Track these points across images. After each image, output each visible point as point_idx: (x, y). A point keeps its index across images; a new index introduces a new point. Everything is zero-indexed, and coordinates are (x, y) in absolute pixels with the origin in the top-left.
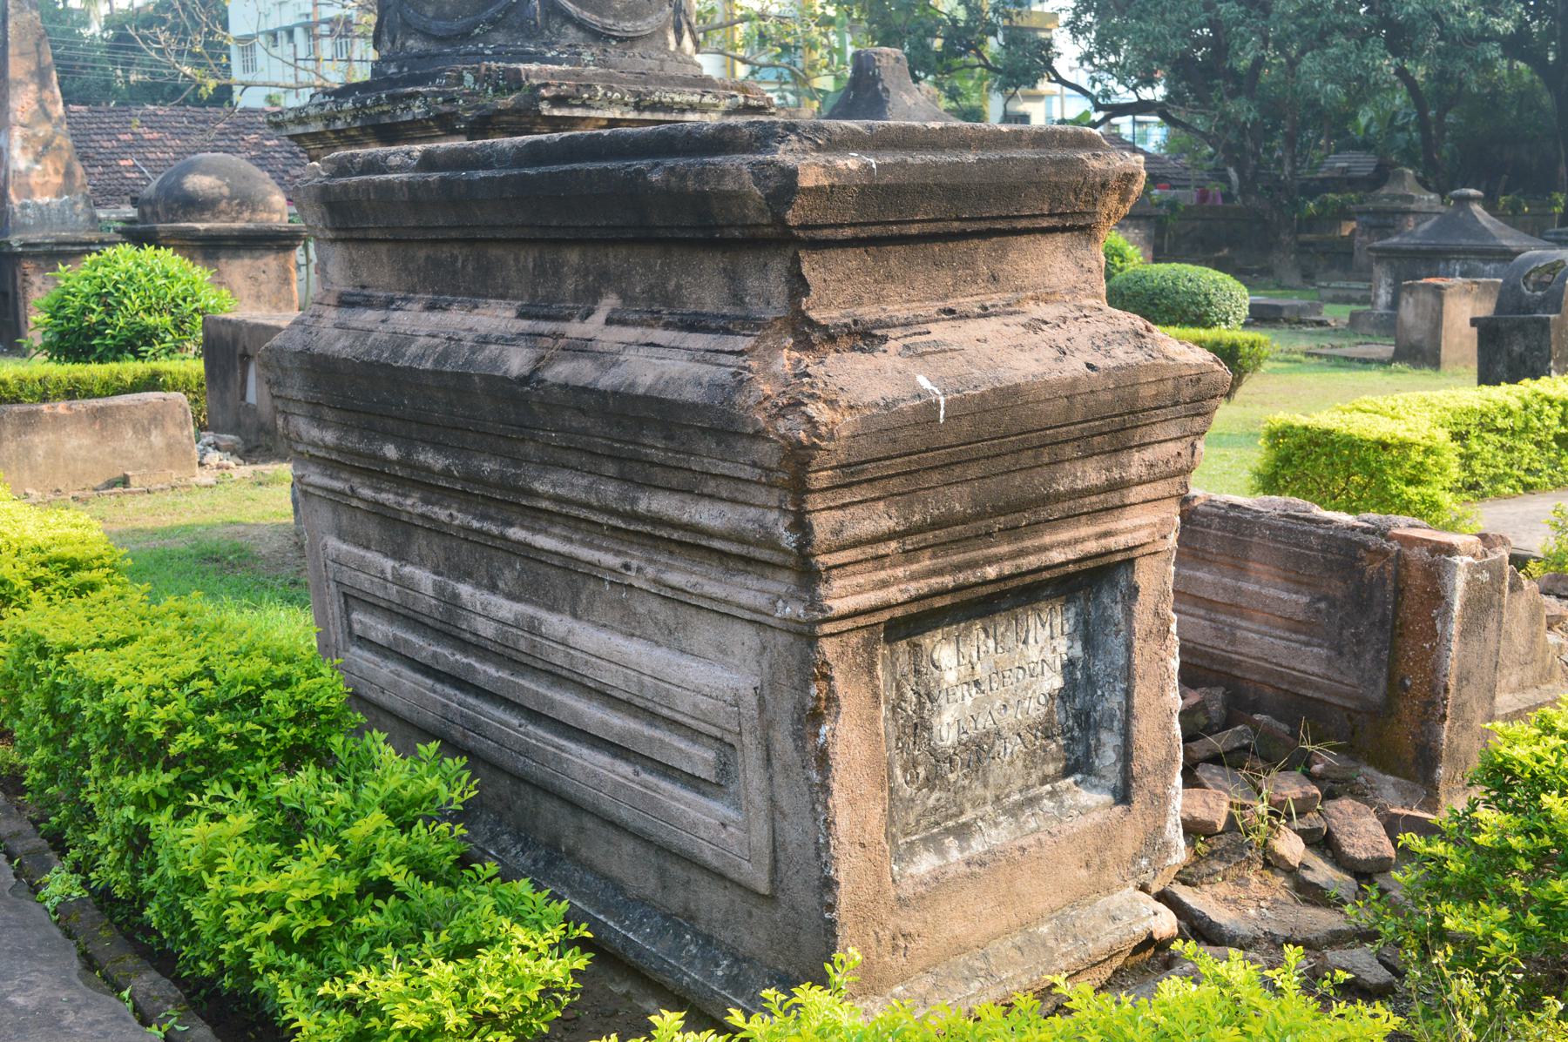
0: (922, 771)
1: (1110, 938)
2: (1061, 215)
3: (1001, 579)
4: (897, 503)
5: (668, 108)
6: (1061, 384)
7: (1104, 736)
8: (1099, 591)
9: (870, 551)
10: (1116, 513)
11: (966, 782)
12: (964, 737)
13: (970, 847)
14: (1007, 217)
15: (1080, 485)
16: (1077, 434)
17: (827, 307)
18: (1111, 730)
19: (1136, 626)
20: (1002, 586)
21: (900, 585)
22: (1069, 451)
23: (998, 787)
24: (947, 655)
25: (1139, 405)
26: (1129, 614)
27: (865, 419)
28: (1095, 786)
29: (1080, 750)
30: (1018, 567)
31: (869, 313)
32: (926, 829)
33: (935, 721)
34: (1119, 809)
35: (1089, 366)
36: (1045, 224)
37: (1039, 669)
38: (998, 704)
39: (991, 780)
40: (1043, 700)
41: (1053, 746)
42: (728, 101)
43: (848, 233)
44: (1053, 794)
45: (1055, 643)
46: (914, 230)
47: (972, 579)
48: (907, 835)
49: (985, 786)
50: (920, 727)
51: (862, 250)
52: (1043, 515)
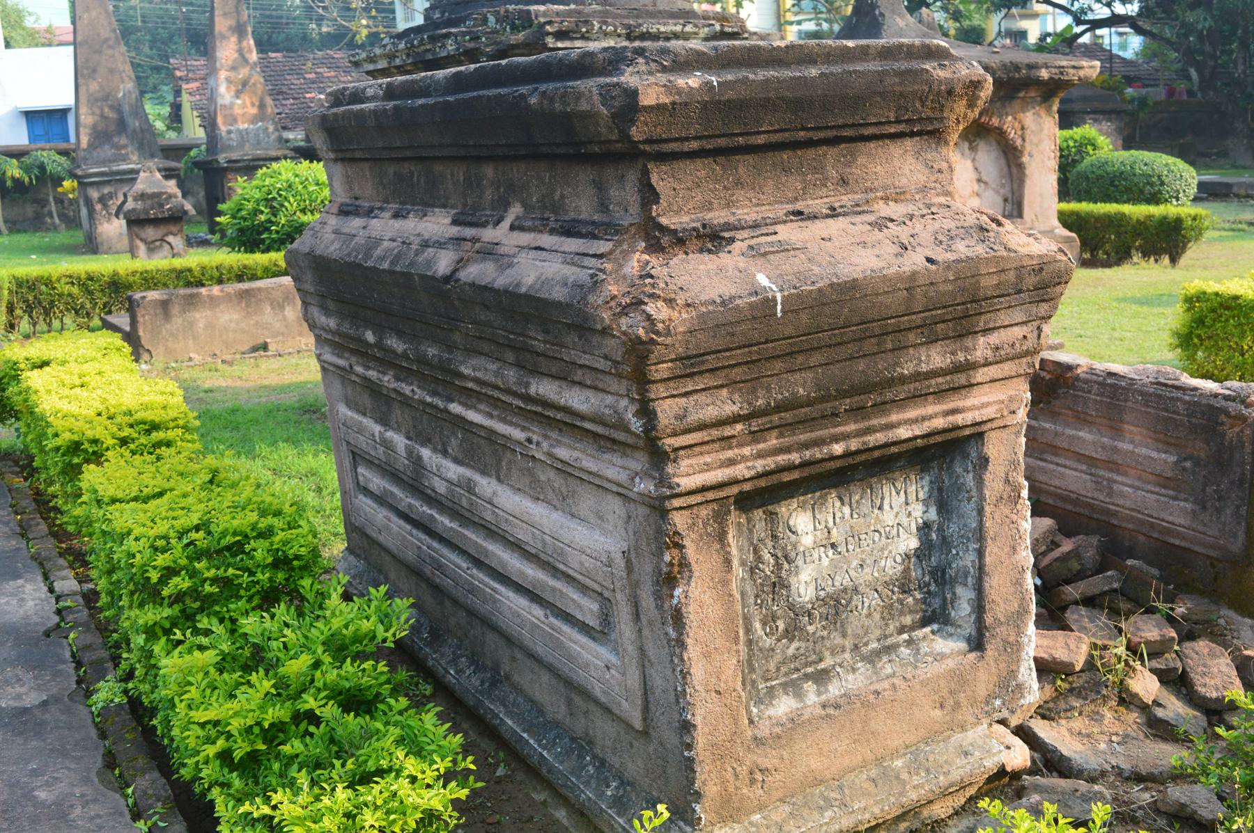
0: (781, 625)
1: (961, 772)
2: (908, 121)
3: (847, 454)
4: (740, 390)
5: (655, 37)
6: (900, 277)
7: (960, 590)
8: (952, 461)
9: (715, 433)
10: (963, 392)
11: (825, 633)
12: (822, 593)
13: (827, 691)
14: (853, 125)
15: (924, 368)
16: (919, 322)
17: (677, 213)
18: (966, 585)
19: (987, 493)
20: (850, 460)
21: (748, 463)
22: (912, 337)
23: (857, 636)
24: (803, 522)
25: (981, 294)
26: (980, 482)
27: (701, 317)
28: (951, 635)
29: (936, 603)
30: (864, 443)
31: (718, 217)
32: (786, 674)
33: (793, 580)
34: (972, 656)
35: (929, 260)
36: (892, 130)
37: (894, 532)
38: (855, 563)
39: (849, 631)
40: (899, 559)
41: (910, 599)
42: (706, 29)
43: (694, 145)
44: (909, 642)
45: (910, 508)
46: (761, 140)
47: (819, 456)
48: (767, 680)
49: (844, 636)
50: (778, 585)
51: (711, 160)
52: (889, 396)
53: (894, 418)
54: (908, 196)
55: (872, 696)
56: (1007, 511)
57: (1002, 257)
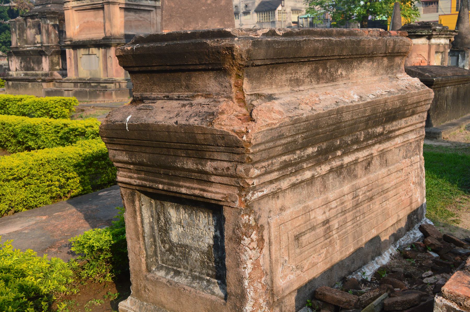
2: (205, 64)
3: (163, 190)
6: (163, 126)
13: (174, 278)
15: (185, 167)
30: (169, 188)
31: (147, 94)
36: (200, 68)
39: (189, 263)
41: (211, 264)
44: (208, 281)
45: (209, 227)
46: (155, 68)
49: (188, 263)
52: (177, 173)
53: (181, 183)
54: (211, 96)
55: (182, 289)
56: (235, 246)
57: (204, 128)
